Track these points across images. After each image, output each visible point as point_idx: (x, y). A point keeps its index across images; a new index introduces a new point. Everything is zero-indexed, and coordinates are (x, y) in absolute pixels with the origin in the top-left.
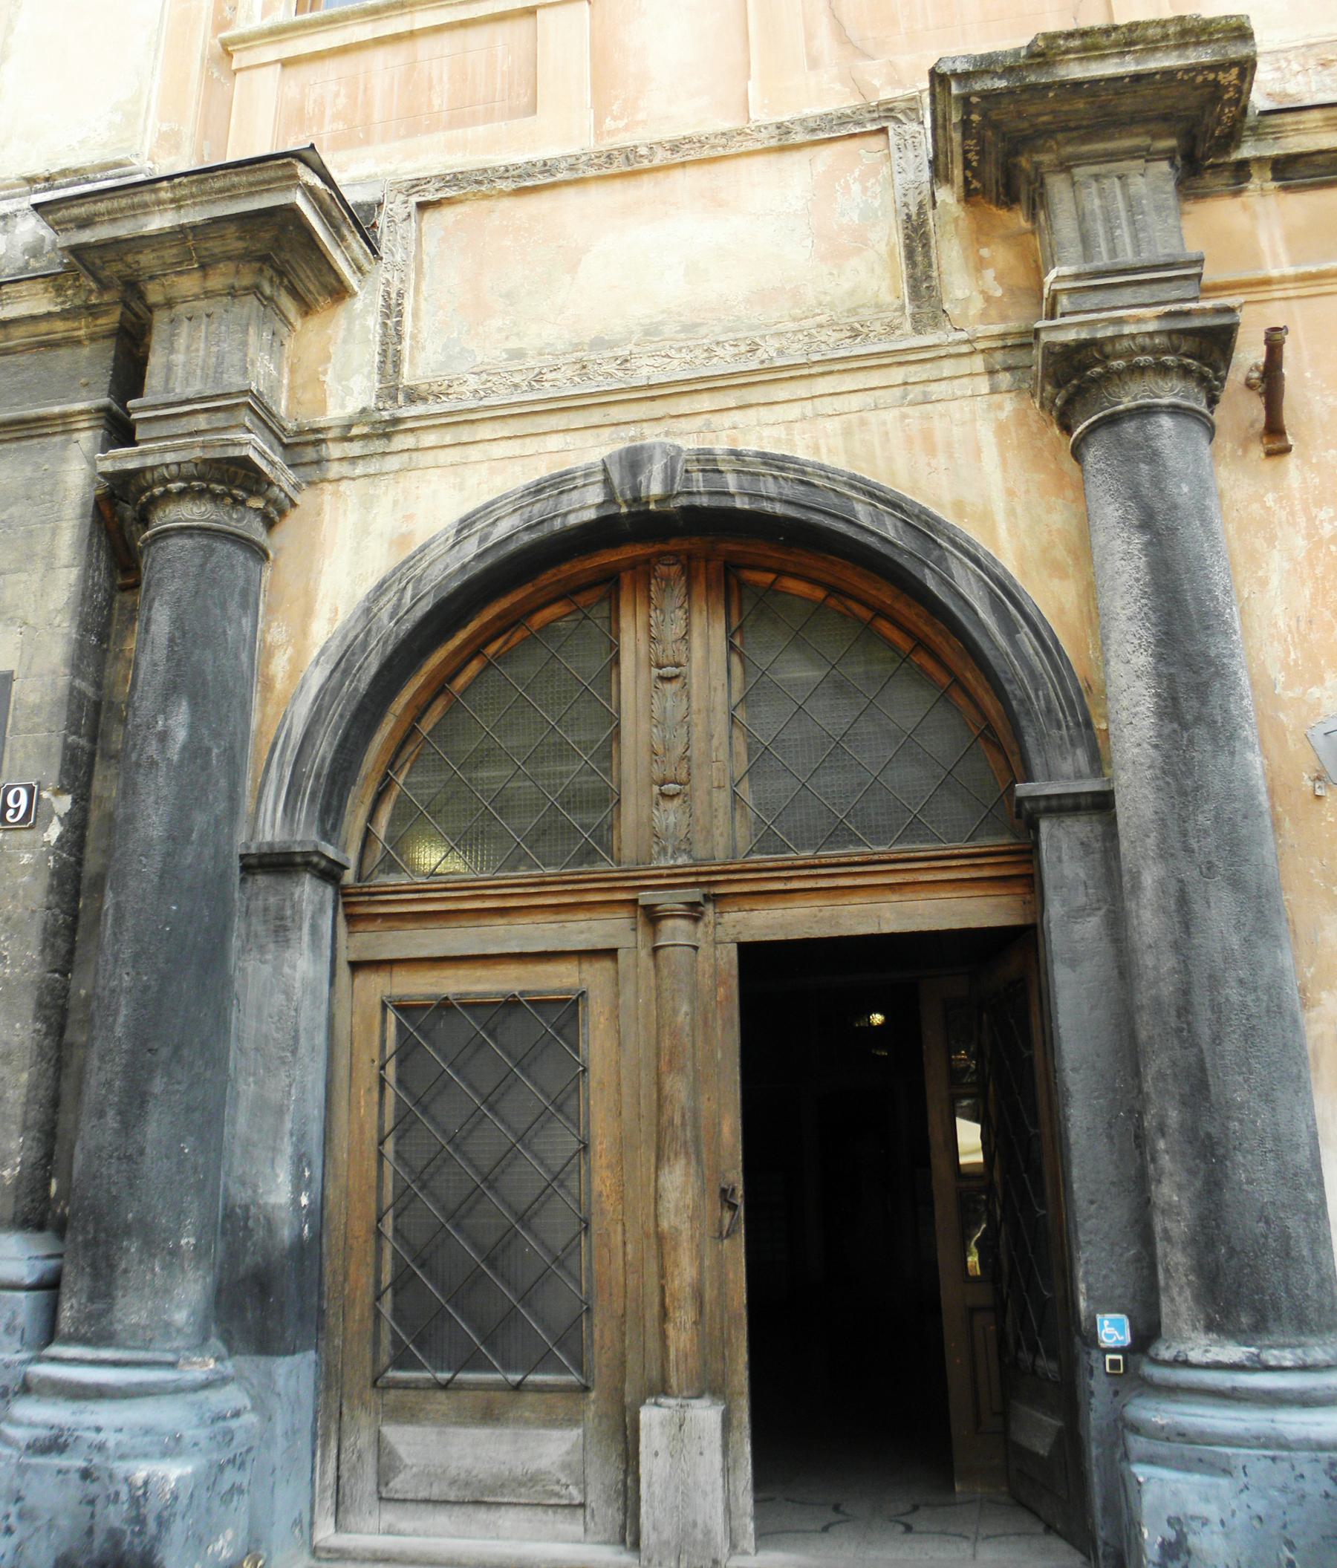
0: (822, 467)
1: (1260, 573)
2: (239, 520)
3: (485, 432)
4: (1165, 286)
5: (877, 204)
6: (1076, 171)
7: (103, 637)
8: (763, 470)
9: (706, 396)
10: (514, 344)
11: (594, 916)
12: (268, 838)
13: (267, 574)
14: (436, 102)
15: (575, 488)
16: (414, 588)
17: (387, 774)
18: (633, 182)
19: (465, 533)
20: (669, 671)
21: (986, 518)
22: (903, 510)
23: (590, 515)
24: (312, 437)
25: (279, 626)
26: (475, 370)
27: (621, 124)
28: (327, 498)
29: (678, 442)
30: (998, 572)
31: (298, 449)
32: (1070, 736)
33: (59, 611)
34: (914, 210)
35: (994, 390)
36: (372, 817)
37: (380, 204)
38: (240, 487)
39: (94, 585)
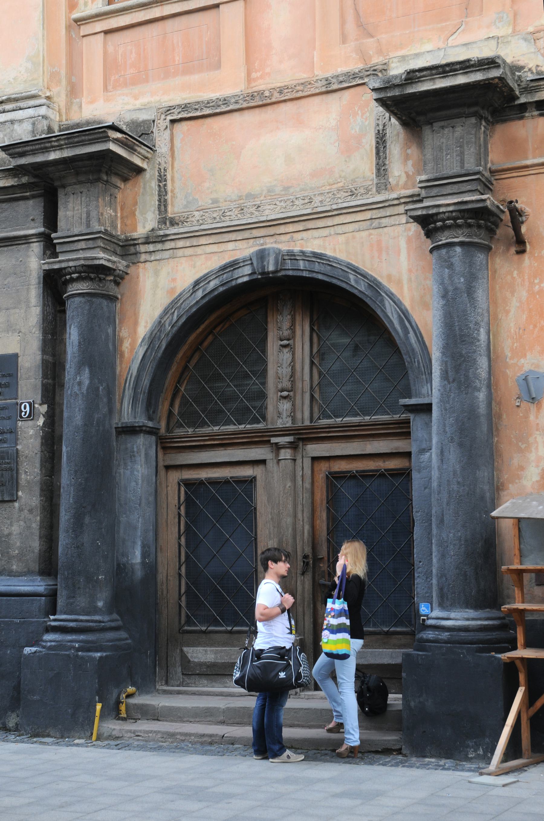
0: (336, 259)
1: (507, 308)
2: (103, 287)
3: (203, 240)
4: (464, 184)
5: (367, 123)
6: (434, 124)
9: (291, 225)
10: (214, 196)
12: (126, 420)
13: (118, 305)
14: (177, 58)
15: (240, 267)
16: (178, 312)
17: (177, 386)
18: (263, 109)
19: (197, 287)
21: (399, 282)
22: (368, 279)
23: (246, 279)
24: (132, 242)
25: (125, 329)
26: (199, 209)
27: (259, 74)
28: (141, 270)
30: (403, 307)
31: (127, 247)
32: (426, 379)
33: (34, 327)
34: (381, 127)
36: (172, 404)
37: (154, 121)
38: (101, 274)
39: (47, 313)
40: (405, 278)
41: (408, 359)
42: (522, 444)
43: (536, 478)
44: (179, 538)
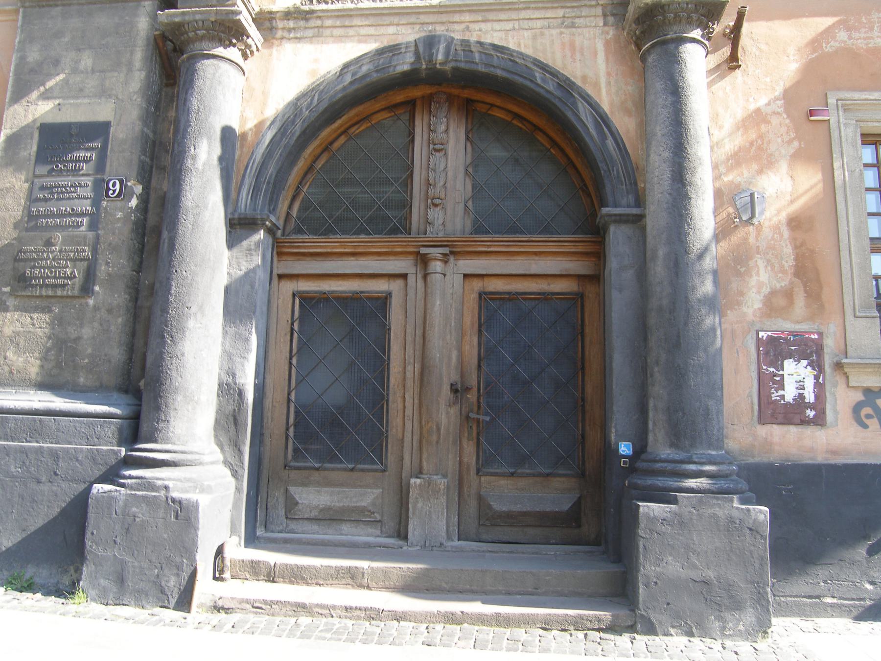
0: (521, 53)
3: (357, 21)
7: (157, 108)
8: (492, 53)
11: (397, 258)
12: (243, 211)
16: (319, 95)
17: (299, 187)
19: (345, 70)
20: (438, 147)
21: (597, 85)
22: (558, 78)
23: (406, 68)
29: (453, 35)
32: (627, 190)
33: (135, 93)
35: (605, 24)
40: (603, 81)
41: (605, 168)
42: (741, 267)
43: (758, 305)
44: (291, 358)
